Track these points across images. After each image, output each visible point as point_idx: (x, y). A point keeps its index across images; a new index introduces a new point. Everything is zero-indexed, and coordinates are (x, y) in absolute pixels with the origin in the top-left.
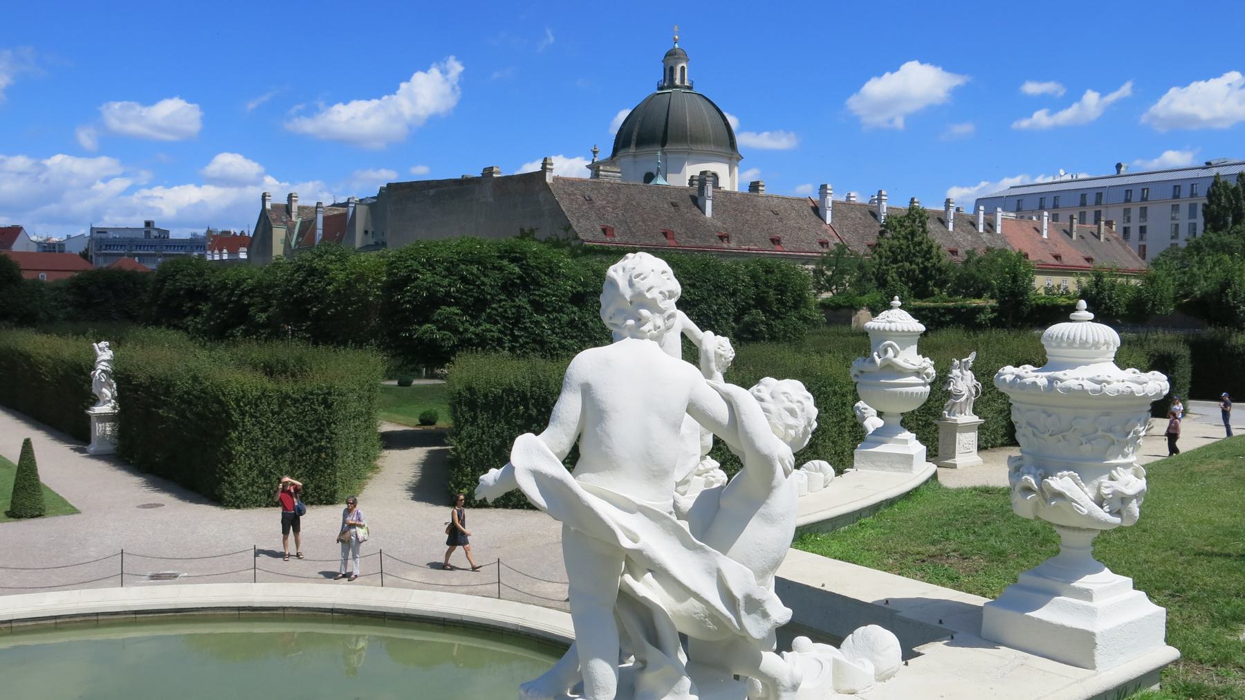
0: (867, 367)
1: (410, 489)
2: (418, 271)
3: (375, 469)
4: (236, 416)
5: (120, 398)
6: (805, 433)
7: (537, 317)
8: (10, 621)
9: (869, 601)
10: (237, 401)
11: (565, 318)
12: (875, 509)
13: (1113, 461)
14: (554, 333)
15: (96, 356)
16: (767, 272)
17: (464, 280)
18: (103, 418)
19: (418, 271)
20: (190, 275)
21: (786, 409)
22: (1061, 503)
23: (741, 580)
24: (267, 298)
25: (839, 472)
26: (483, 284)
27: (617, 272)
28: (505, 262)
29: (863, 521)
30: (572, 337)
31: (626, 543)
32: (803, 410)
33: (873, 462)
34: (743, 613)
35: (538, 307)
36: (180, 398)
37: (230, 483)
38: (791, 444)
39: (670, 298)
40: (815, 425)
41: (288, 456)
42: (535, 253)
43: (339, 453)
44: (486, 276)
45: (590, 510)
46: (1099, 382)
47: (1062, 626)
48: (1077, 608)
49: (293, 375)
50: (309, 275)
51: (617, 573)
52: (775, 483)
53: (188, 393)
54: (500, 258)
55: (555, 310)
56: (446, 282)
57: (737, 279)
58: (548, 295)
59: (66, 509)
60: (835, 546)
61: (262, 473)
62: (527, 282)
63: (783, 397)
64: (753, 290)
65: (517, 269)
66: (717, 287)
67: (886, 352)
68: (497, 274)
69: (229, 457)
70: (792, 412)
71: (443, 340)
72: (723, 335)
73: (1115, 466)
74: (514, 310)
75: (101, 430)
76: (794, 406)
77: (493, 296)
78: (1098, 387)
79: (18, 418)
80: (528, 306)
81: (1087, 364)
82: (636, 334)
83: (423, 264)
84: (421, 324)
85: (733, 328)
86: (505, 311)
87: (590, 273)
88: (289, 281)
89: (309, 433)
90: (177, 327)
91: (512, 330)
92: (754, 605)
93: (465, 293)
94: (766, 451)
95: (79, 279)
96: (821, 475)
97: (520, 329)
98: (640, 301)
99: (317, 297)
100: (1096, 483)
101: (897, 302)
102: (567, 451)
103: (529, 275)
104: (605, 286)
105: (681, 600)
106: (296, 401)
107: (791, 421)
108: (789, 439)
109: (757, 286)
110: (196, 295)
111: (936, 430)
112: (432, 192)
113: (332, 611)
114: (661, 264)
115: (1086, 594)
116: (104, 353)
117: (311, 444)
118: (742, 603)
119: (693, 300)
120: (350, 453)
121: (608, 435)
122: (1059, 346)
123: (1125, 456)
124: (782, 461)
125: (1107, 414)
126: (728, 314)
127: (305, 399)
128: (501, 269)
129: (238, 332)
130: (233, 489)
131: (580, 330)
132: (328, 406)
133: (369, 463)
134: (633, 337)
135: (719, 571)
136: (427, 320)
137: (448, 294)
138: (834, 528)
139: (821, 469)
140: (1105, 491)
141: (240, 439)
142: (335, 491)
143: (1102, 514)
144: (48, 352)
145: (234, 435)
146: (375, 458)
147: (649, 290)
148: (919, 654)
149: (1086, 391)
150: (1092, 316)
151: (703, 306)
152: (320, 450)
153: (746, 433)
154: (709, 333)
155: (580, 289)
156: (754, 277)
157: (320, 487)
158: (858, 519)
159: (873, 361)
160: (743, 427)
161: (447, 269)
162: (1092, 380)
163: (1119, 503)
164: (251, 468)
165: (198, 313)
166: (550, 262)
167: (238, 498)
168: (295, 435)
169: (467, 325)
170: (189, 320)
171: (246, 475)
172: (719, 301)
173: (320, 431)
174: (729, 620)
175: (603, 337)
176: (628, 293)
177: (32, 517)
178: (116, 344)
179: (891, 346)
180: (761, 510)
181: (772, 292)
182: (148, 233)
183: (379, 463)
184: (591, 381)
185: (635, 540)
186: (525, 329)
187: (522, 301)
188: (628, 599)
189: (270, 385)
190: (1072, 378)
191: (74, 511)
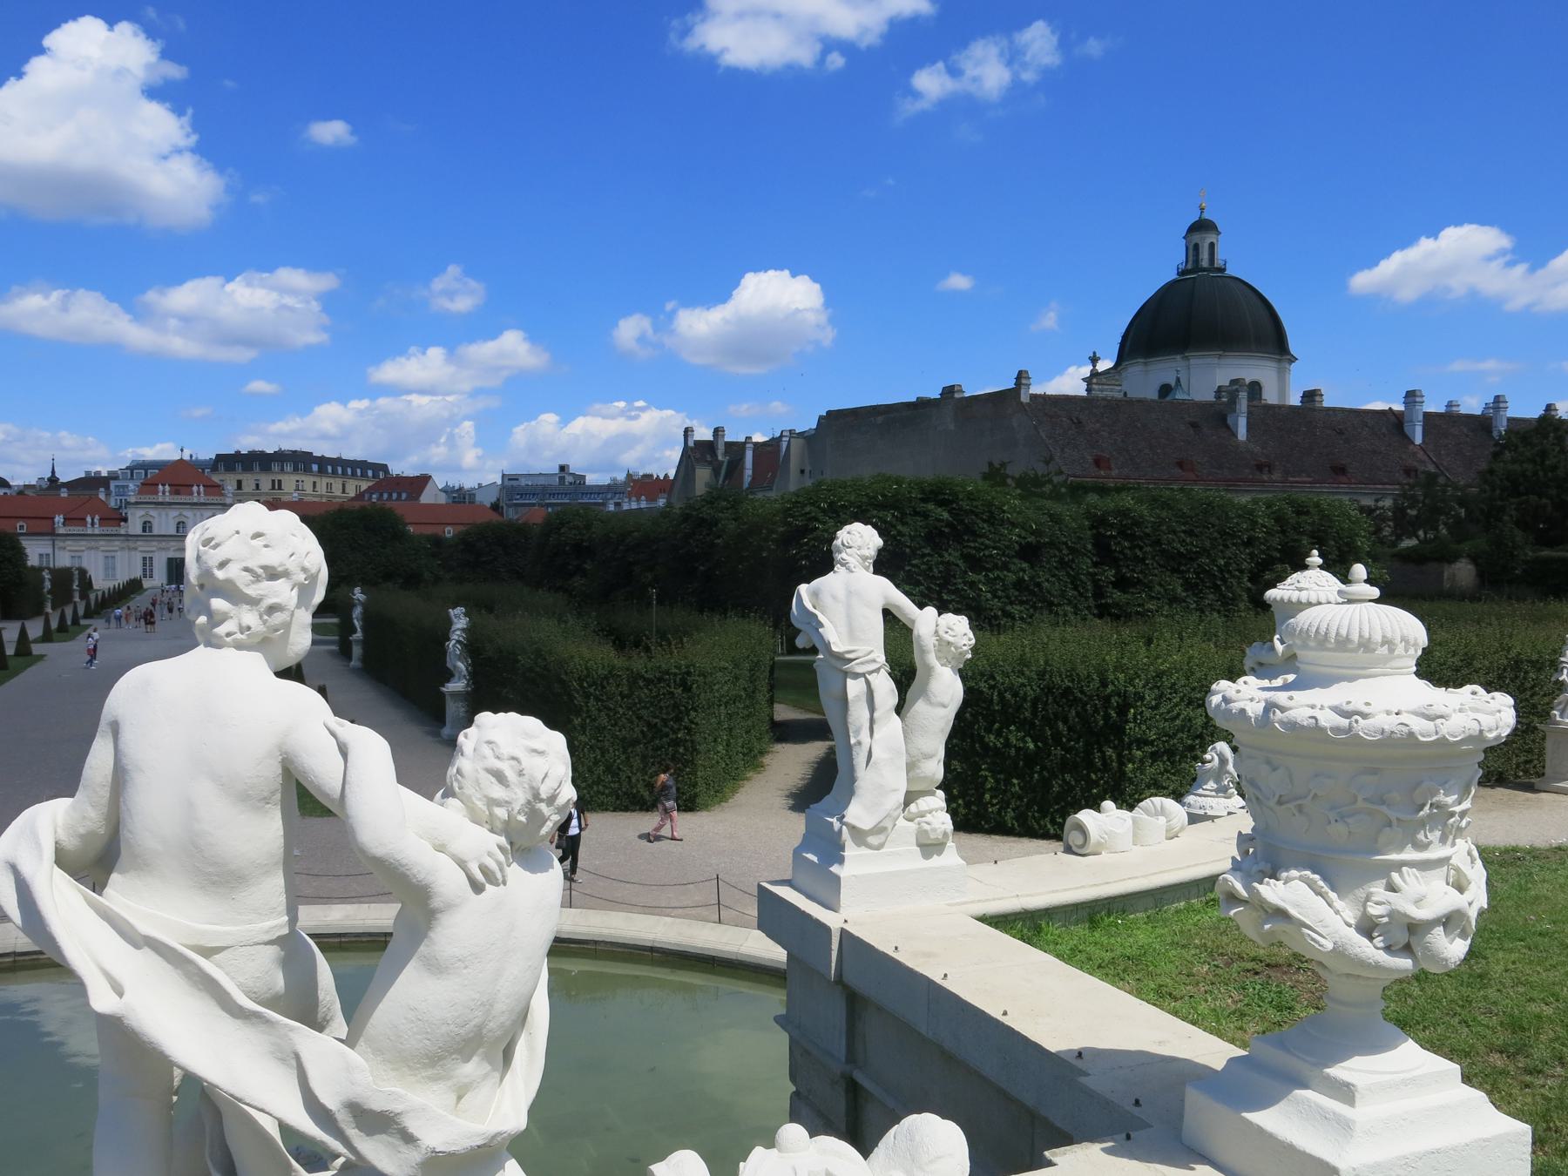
0: (1265, 658)
1: (792, 795)
2: (816, 519)
3: (758, 767)
4: (579, 699)
7: (971, 576)
10: (580, 680)
11: (1011, 577)
13: (1394, 857)
14: (995, 596)
15: (450, 623)
16: (1299, 513)
22: (1281, 926)
26: (900, 533)
28: (931, 506)
30: (1022, 603)
32: (521, 774)
34: (352, 1133)
35: (975, 563)
41: (640, 748)
42: (970, 493)
43: (702, 748)
44: (904, 524)
46: (1347, 714)
47: (1290, 1149)
48: (1325, 1116)
54: (923, 500)
55: (996, 567)
58: (987, 547)
61: (608, 769)
62: (960, 531)
63: (486, 750)
64: (1275, 541)
65: (946, 515)
66: (1223, 533)
68: (920, 522)
70: (499, 777)
73: (1399, 866)
74: (941, 568)
77: (913, 551)
78: (1344, 722)
80: (960, 563)
81: (1351, 679)
85: (1249, 589)
86: (930, 569)
89: (665, 722)
91: (939, 593)
96: (1162, 820)
97: (950, 592)
100: (1361, 893)
101: (1315, 558)
103: (962, 522)
106: (648, 682)
107: (498, 792)
108: (499, 825)
109: (1283, 532)
111: (1544, 738)
112: (880, 419)
113: (652, 949)
115: (1345, 1092)
116: (460, 621)
117: (667, 735)
119: (1190, 551)
120: (720, 748)
122: (1305, 646)
123: (1423, 847)
125: (1374, 771)
126: (1241, 571)
127: (660, 680)
128: (925, 515)
131: (1032, 593)
133: (752, 759)
135: (297, 1057)
139: (1162, 812)
140: (1374, 910)
142: (696, 795)
143: (1370, 950)
146: (762, 753)
147: (222, 565)
148: (1050, 1164)
149: (1323, 730)
150: (1375, 592)
151: (1204, 560)
152: (676, 743)
154: (931, 611)
155: (1031, 539)
156: (1279, 519)
159: (1273, 648)
162: (1337, 710)
163: (1407, 934)
164: (596, 763)
166: (991, 504)
168: (649, 724)
170: (578, 582)
171: (590, 771)
172: (1228, 553)
173: (678, 719)
178: (475, 606)
182: (562, 479)
183: (766, 760)
185: (119, 991)
186: (956, 592)
187: (952, 555)
189: (619, 662)
190: (1310, 706)
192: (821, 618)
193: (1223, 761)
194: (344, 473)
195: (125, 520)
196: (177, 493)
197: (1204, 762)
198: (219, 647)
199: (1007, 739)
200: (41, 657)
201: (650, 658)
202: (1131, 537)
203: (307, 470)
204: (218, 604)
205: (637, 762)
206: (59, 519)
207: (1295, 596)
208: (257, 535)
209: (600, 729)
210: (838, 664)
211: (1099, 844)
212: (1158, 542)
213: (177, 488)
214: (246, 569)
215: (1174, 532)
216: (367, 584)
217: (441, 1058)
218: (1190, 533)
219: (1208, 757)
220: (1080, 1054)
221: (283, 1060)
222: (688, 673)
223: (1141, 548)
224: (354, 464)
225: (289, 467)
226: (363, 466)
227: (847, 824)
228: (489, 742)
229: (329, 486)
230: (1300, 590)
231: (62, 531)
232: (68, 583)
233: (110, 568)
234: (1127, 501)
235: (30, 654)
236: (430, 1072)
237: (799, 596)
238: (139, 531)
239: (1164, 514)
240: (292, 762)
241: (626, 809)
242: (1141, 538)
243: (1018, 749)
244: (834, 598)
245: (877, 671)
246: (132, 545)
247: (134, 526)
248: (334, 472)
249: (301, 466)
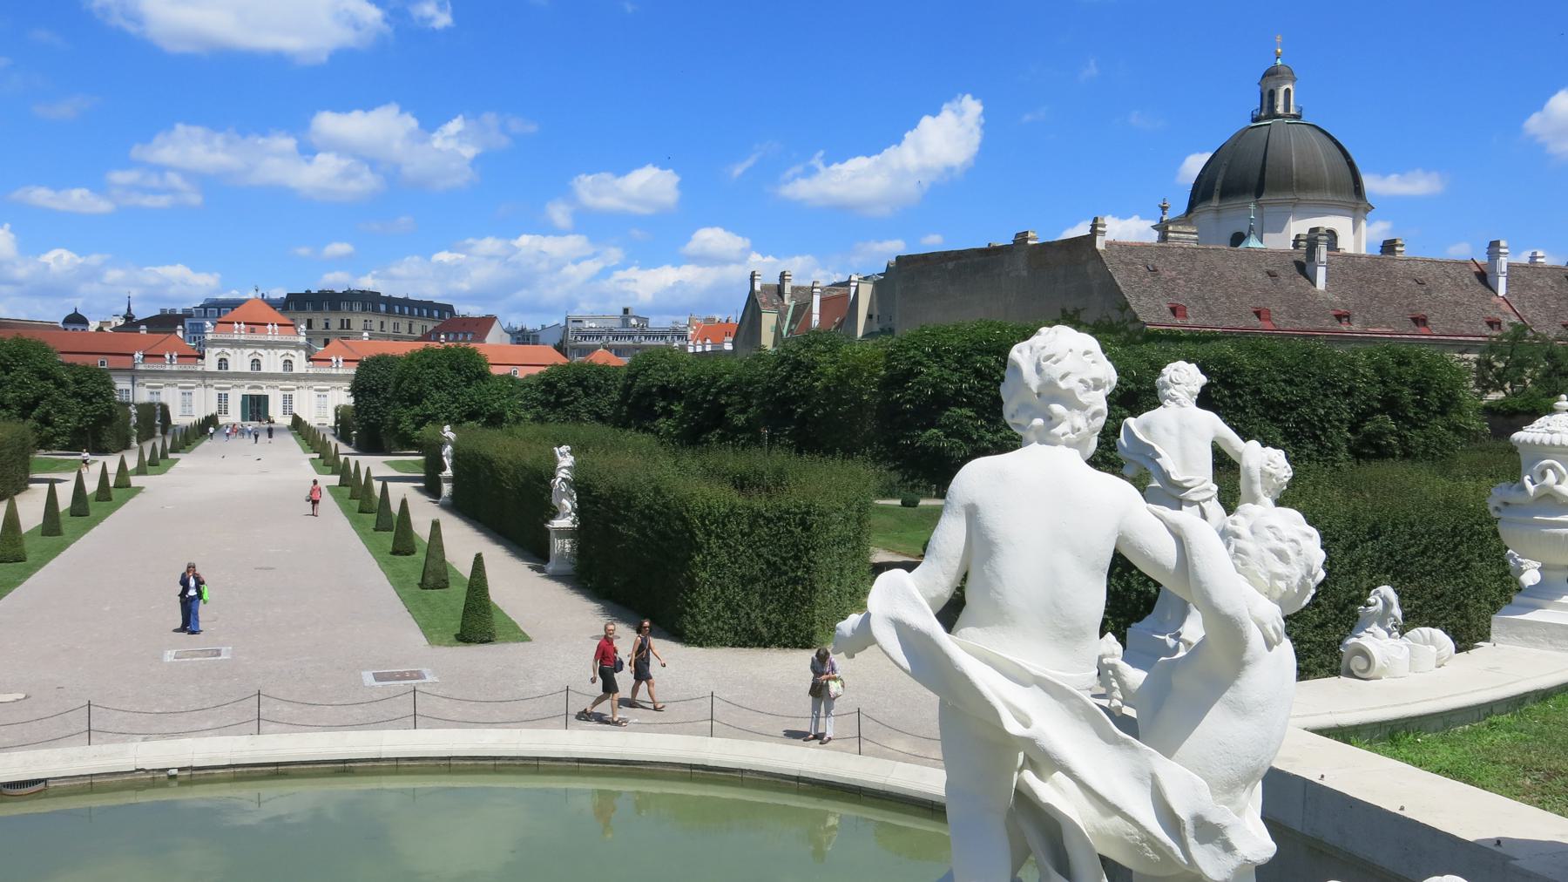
0: (1513, 497)
2: (921, 364)
4: (700, 537)
5: (580, 512)
6: (1303, 586)
8: (449, 758)
9: (1471, 837)
10: (702, 518)
12: (1517, 703)
15: (556, 461)
16: (1399, 364)
17: (978, 373)
18: (562, 533)
19: (921, 364)
20: (663, 369)
21: (1272, 550)
23: (1188, 791)
24: (747, 397)
25: (1458, 650)
27: (1021, 354)
29: (1494, 719)
31: (1013, 727)
32: (1299, 553)
33: (1520, 636)
34: (1191, 841)
36: (641, 512)
37: (693, 616)
38: (1280, 602)
39: (1096, 388)
40: (1322, 575)
41: (759, 586)
43: (819, 586)
45: (964, 677)
49: (768, 489)
50: (794, 369)
51: (1010, 767)
52: (1248, 656)
53: (648, 507)
56: (956, 378)
57: (1355, 373)
59: (517, 635)
60: (1444, 754)
61: (728, 605)
63: (1269, 534)
64: (1376, 391)
66: (1324, 383)
67: (1543, 475)
69: (692, 584)
70: (1281, 556)
71: (952, 449)
72: (1275, 447)
75: (561, 547)
76: (1285, 546)
79: (479, 530)
82: (1046, 438)
83: (928, 355)
84: (924, 429)
85: (1348, 440)
87: (1146, 366)
88: (771, 376)
89: (784, 560)
90: (646, 430)
92: (1210, 832)
93: (980, 391)
94: (1229, 610)
95: (549, 374)
96: (1433, 649)
98: (1051, 392)
99: (802, 396)
102: (947, 596)
104: (1007, 373)
105: (1106, 815)
106: (769, 520)
107: (1280, 568)
108: (1277, 595)
109: (1384, 383)
110: (667, 393)
112: (951, 265)
113: (798, 779)
114: (1089, 342)
116: (565, 459)
117: (786, 573)
118: (1189, 827)
121: (998, 576)
124: (1261, 626)
126: (1341, 421)
127: (780, 519)
129: (713, 436)
130: (696, 623)
132: (807, 528)
134: (1041, 442)
135: (1154, 777)
136: (932, 425)
137: (959, 392)
138: (1446, 726)
139: (1432, 641)
141: (704, 564)
142: (813, 633)
144: (509, 456)
145: (697, 559)
147: (1063, 377)
151: (1304, 410)
152: (796, 581)
153: (1199, 582)
154: (1254, 444)
155: (1132, 386)
157: (795, 627)
158: (1487, 715)
159: (1523, 488)
160: (1195, 573)
161: (958, 361)
164: (716, 600)
165: (669, 414)
167: (700, 634)
168: (768, 562)
169: (982, 431)
170: (663, 424)
172: (1328, 404)
173: (797, 558)
174: (1170, 848)
175: (1008, 442)
176: (1034, 382)
177: (482, 642)
179: (1552, 467)
180: (1228, 694)
181: (1406, 391)
182: (625, 322)
184: (978, 502)
188: (1025, 801)
189: (739, 501)
191: (525, 638)
192: (1158, 448)
193: (1387, 604)
194: (411, 313)
195: (202, 357)
196: (253, 331)
197: (1368, 605)
198: (1054, 444)
199: (1128, 583)
200: (139, 489)
201: (770, 498)
202: (1232, 386)
203: (376, 310)
204: (1057, 408)
205: (756, 599)
207: (1547, 439)
208: (1086, 353)
209: (721, 566)
210: (1174, 492)
211: (1382, 669)
212: (1258, 391)
214: (1082, 381)
215: (1275, 381)
216: (456, 424)
217: (1237, 785)
218: (1290, 382)
219: (1371, 600)
220: (1499, 842)
221: (1141, 780)
222: (808, 513)
223: (1241, 397)
225: (357, 307)
226: (430, 306)
227: (1183, 641)
228: (1270, 527)
229: (396, 326)
230: (1552, 432)
231: (141, 367)
232: (154, 418)
233: (186, 405)
234: (1228, 349)
235: (129, 486)
236: (1227, 797)
237: (1128, 428)
238: (215, 369)
239: (1264, 363)
240: (1127, 539)
241: (744, 645)
242: (1241, 387)
243: (1139, 593)
244: (1166, 430)
245: (1209, 499)
246: (208, 382)
248: (401, 312)
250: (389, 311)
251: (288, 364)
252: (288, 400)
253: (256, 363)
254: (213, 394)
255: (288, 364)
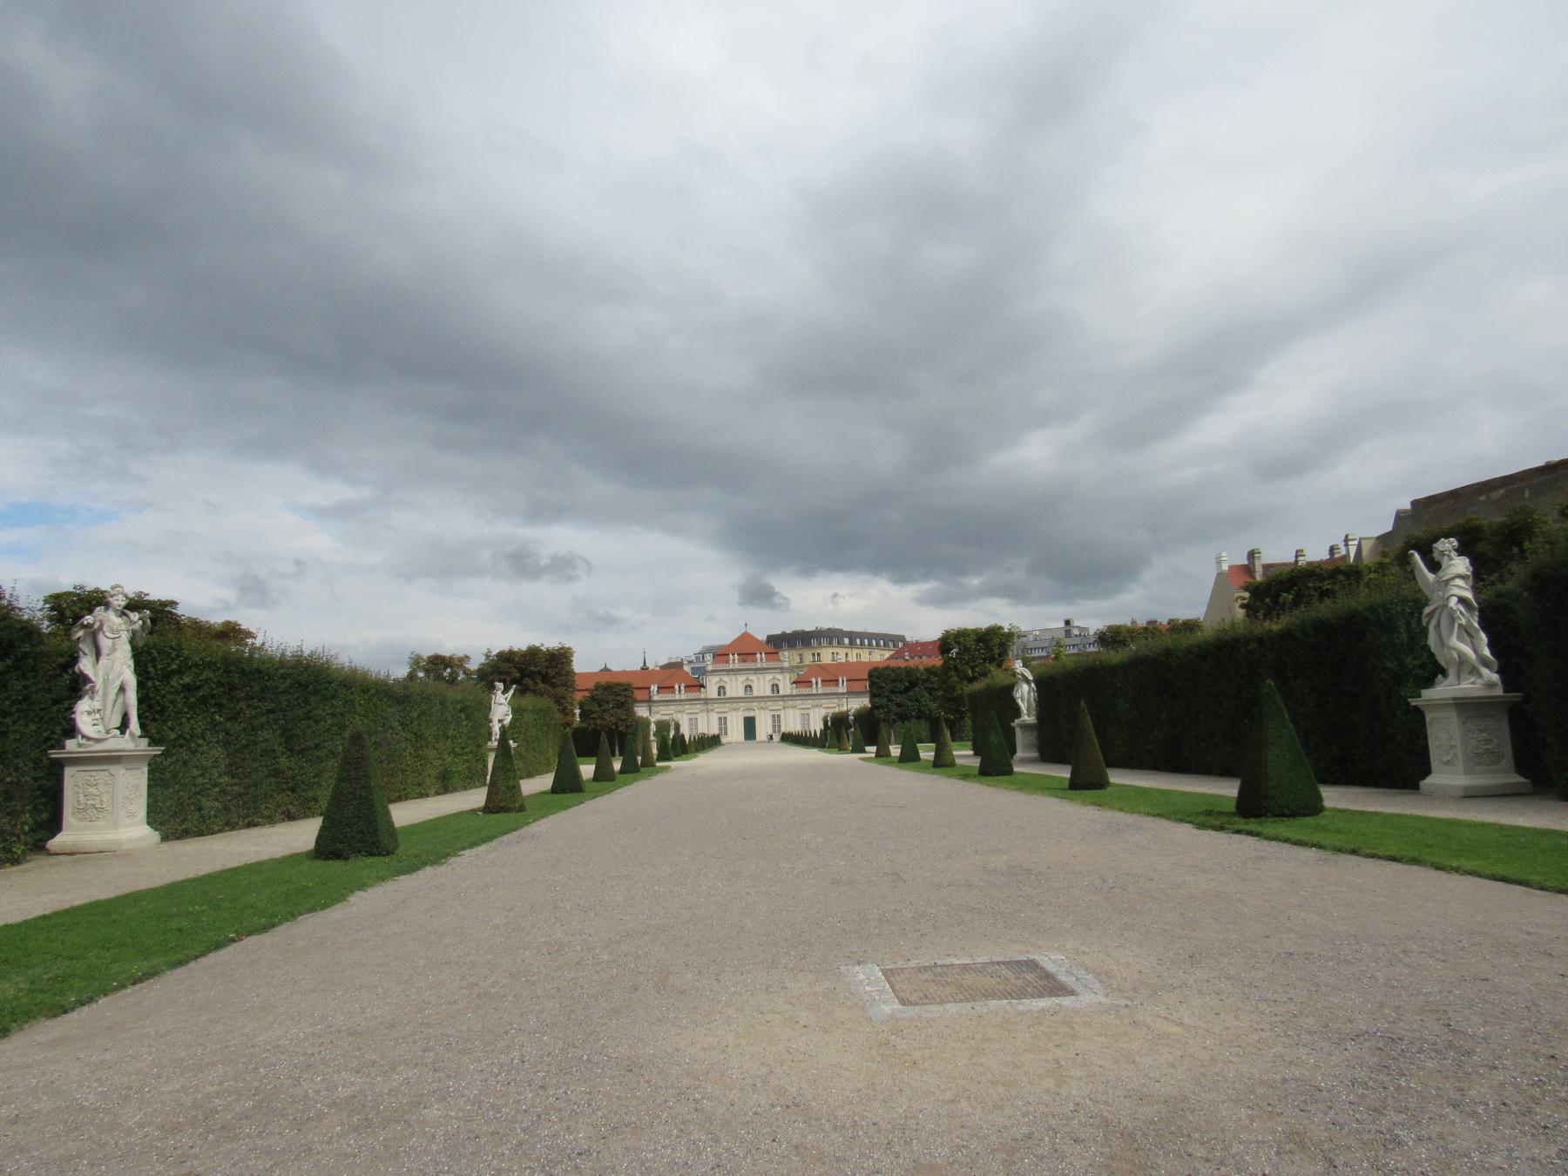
112: (1495, 495)
182: (1068, 633)
194: (870, 644)
203: (840, 643)
206: (654, 688)
213: (746, 656)
224: (878, 637)
225: (824, 642)
229: (858, 656)
233: (693, 722)
238: (714, 694)
247: (711, 691)
248: (862, 644)
249: (835, 642)
250: (852, 643)
251: (775, 687)
252: (776, 719)
253: (749, 688)
254: (714, 717)
255: (775, 687)
